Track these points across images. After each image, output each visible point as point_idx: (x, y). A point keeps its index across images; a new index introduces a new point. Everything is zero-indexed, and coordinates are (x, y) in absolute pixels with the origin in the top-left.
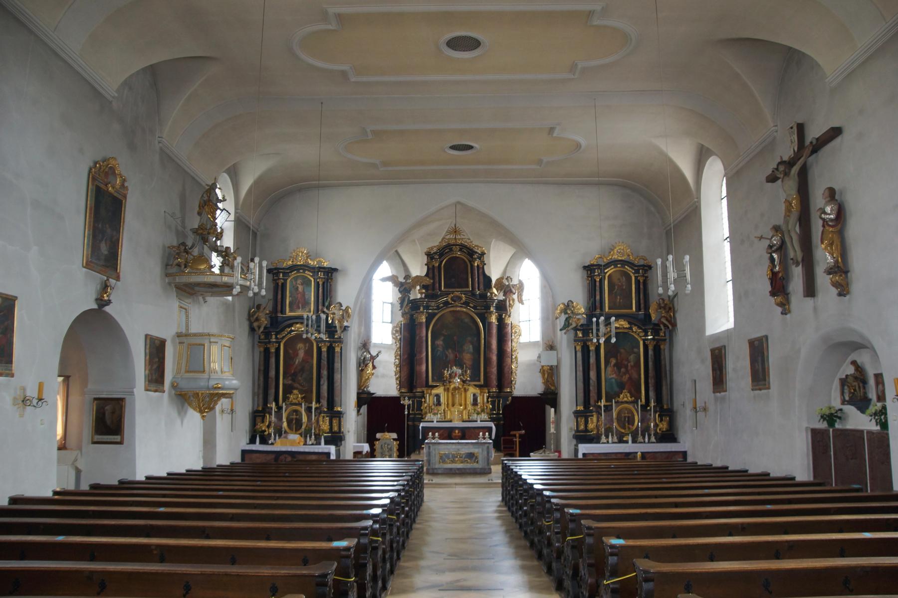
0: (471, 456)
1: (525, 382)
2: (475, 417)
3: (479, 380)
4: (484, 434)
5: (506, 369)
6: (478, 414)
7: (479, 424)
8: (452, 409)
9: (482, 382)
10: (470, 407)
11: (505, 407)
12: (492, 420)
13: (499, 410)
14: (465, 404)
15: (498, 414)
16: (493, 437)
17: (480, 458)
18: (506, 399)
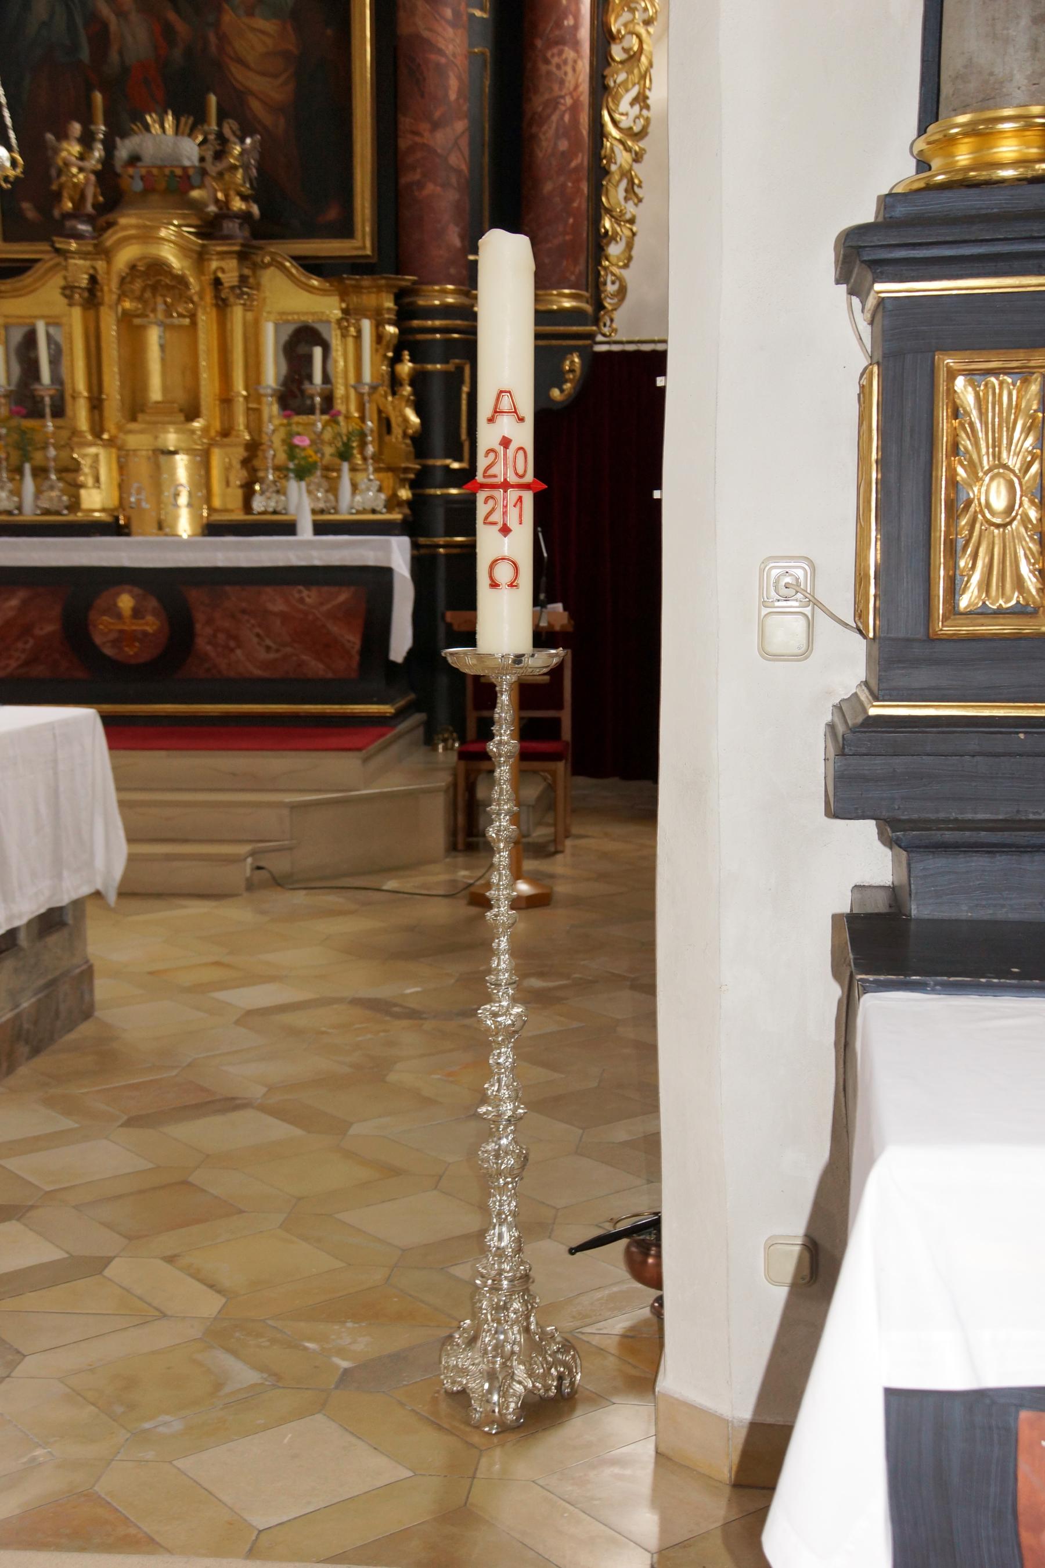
3: (345, 229)
7: (306, 549)
8: (137, 440)
9: (362, 242)
14: (226, 401)
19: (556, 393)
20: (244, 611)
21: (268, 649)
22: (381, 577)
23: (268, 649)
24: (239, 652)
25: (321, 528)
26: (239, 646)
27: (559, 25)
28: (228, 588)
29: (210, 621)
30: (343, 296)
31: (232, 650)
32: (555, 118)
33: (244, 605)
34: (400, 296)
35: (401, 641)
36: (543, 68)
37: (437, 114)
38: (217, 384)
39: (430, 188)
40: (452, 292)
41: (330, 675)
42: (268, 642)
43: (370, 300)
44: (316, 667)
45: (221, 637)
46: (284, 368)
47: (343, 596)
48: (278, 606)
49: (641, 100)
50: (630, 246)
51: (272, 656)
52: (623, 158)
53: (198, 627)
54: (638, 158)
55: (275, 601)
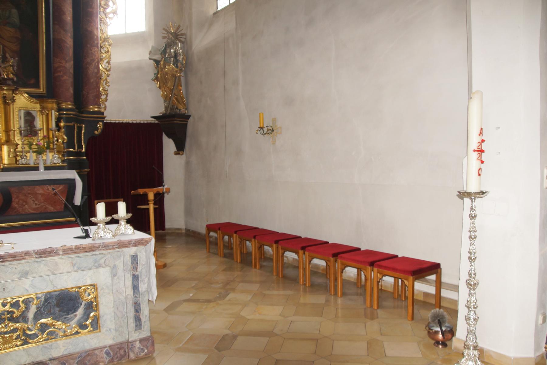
0: (63, 303)
1: (128, 97)
2: (31, 158)
3: (37, 86)
4: (111, 210)
5: (91, 70)
6: (39, 152)
9: (42, 89)
10: (18, 139)
11: (92, 141)
12: (71, 166)
13: (80, 147)
15: (78, 154)
16: (78, 200)
17: (106, 308)
18: (92, 125)
19: (96, 132)
20: (29, 194)
21: (36, 204)
22: (73, 181)
23: (36, 204)
24: (26, 206)
25: (47, 168)
26: (26, 204)
27: (94, 42)
28: (24, 187)
29: (17, 197)
30: (41, 103)
31: (24, 206)
32: (94, 64)
33: (29, 192)
34: (58, 104)
35: (78, 200)
36: (90, 52)
37: (67, 59)
38: (4, 127)
39: (65, 77)
40: (70, 105)
41: (55, 211)
42: (36, 202)
43: (50, 105)
44: (51, 209)
45: (21, 202)
46: (35, 123)
47: (61, 187)
48: (41, 191)
49: (108, 62)
50: (107, 97)
51: (37, 206)
52: (104, 75)
53: (13, 199)
54: (108, 76)
55: (40, 190)
